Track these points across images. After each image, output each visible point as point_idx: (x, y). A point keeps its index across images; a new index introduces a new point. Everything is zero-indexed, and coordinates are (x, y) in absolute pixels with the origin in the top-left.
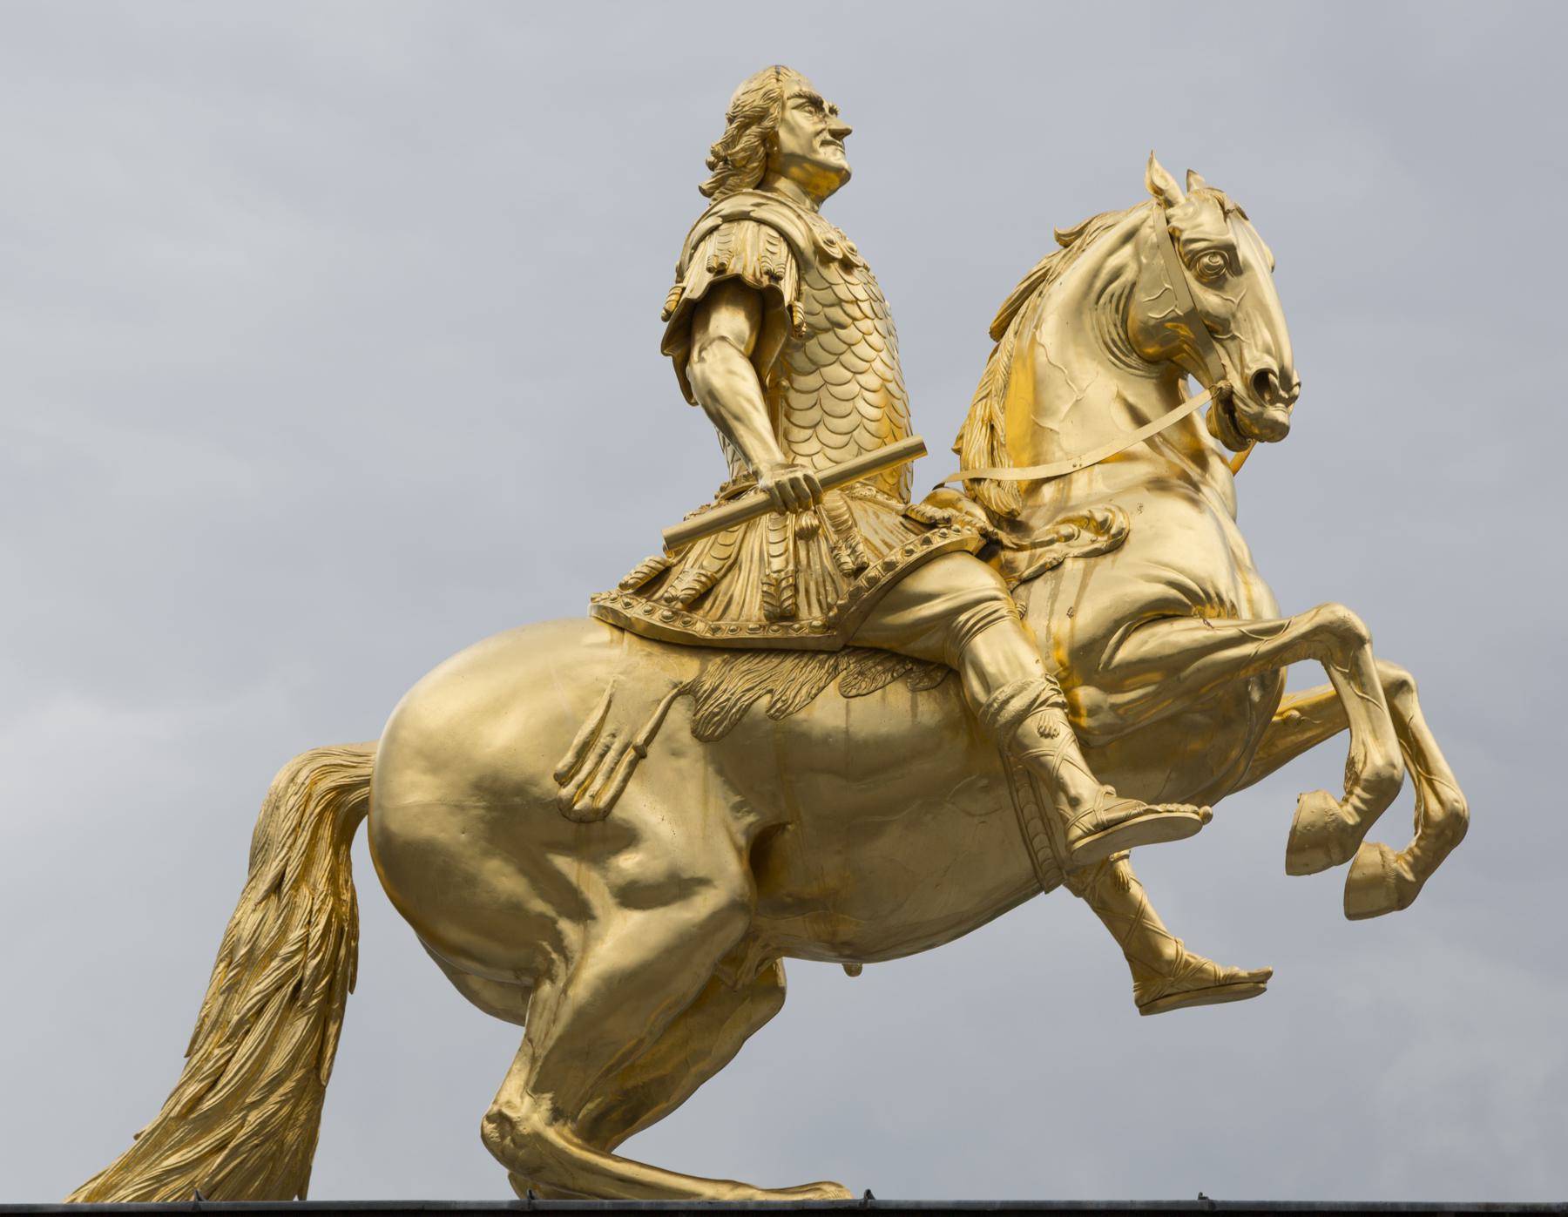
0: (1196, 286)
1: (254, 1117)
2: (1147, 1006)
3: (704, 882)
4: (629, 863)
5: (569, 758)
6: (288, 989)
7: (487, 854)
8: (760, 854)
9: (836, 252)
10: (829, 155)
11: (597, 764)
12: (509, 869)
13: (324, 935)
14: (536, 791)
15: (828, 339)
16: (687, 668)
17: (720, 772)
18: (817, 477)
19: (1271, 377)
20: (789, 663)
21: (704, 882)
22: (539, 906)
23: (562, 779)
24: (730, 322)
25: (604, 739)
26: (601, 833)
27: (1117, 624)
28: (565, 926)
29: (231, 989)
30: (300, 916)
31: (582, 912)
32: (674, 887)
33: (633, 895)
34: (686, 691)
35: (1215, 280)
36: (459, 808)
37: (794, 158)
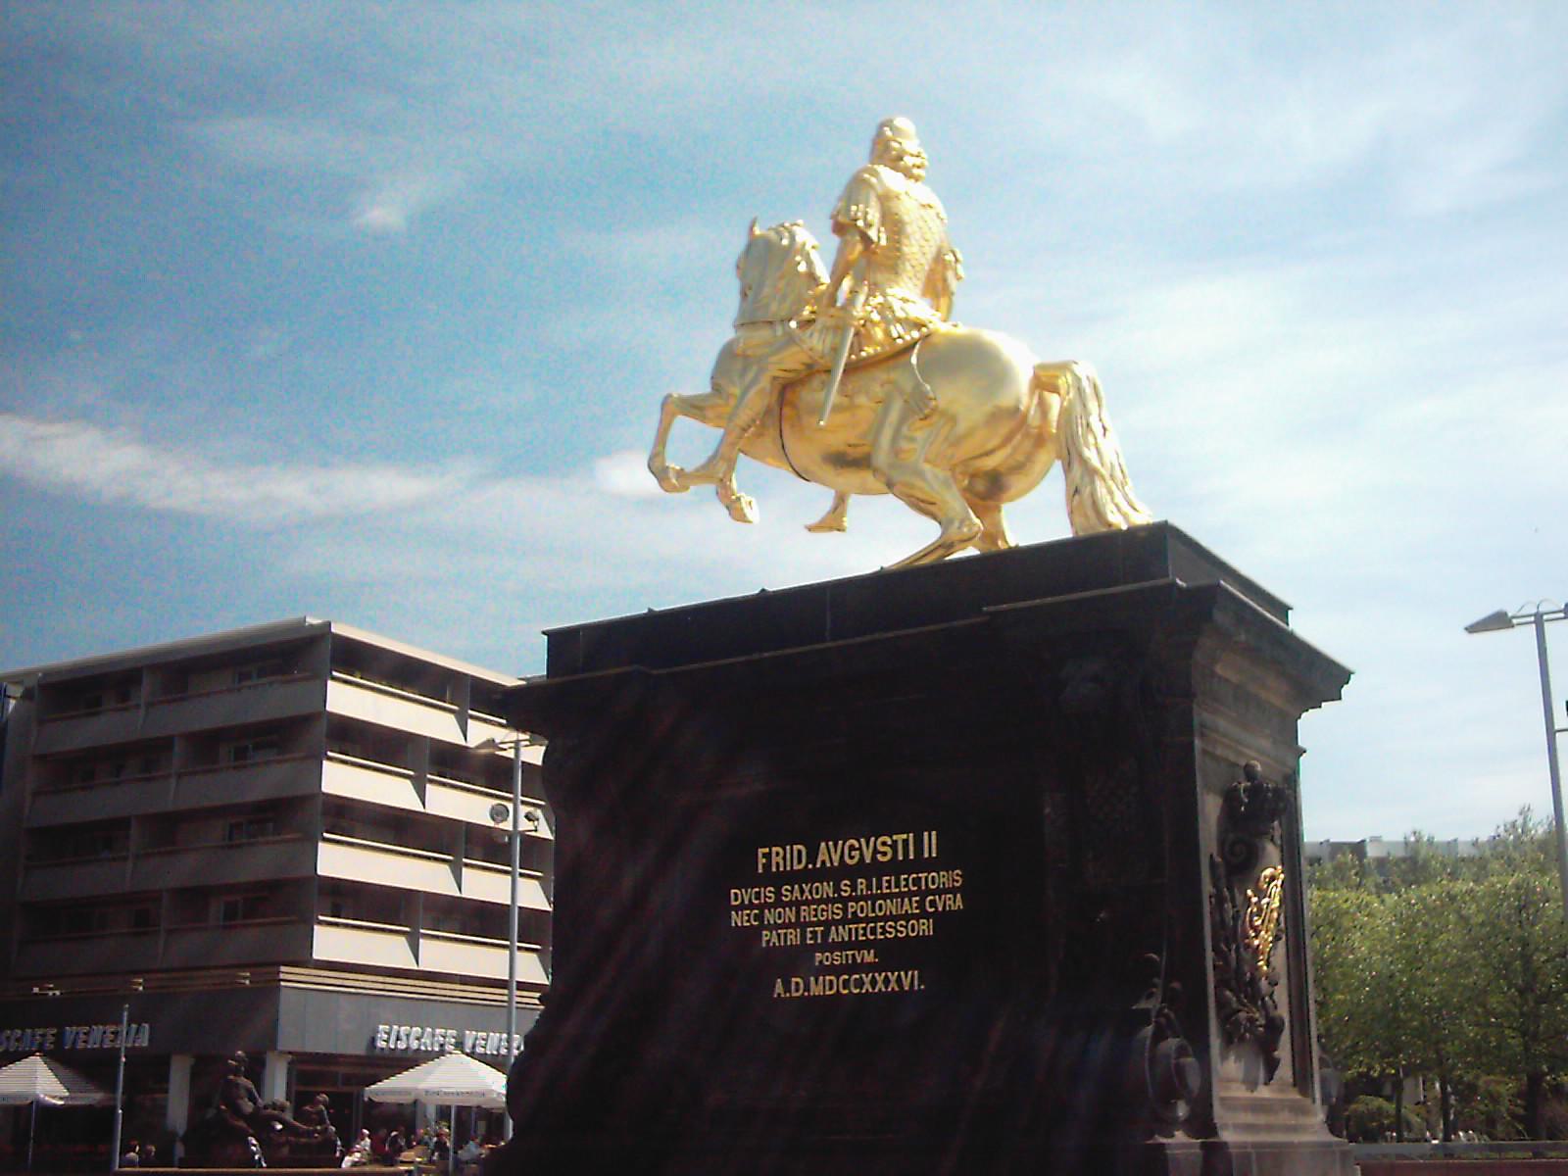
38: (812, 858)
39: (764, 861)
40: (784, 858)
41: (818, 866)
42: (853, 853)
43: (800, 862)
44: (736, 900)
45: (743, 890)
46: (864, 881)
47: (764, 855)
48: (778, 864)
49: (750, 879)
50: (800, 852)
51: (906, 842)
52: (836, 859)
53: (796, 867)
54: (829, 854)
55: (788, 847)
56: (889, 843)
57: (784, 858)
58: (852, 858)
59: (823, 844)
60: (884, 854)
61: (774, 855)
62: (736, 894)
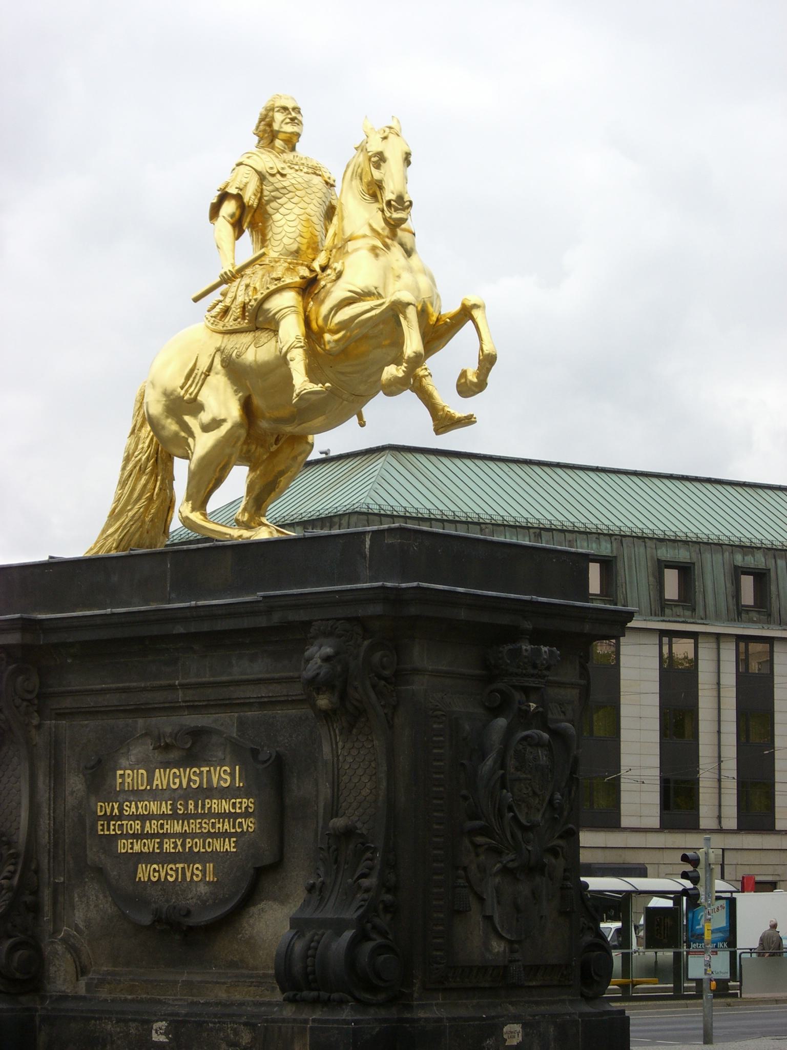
0: (372, 168)
1: (131, 514)
2: (437, 434)
3: (224, 420)
4: (205, 417)
5: (183, 380)
6: (138, 468)
7: (167, 417)
8: (247, 406)
9: (275, 171)
10: (289, 128)
11: (193, 382)
12: (174, 422)
13: (149, 447)
14: (176, 393)
15: (274, 204)
16: (218, 341)
17: (229, 379)
18: (234, 271)
19: (393, 203)
20: (243, 334)
21: (224, 420)
22: (183, 434)
23: (182, 388)
24: (229, 208)
25: (196, 371)
26: (195, 407)
27: (332, 309)
28: (190, 440)
29: (124, 468)
30: (141, 441)
31: (192, 434)
32: (215, 424)
33: (206, 428)
34: (218, 350)
35: (378, 166)
36: (158, 401)
37: (278, 132)
38: (150, 781)
39: (120, 781)
42: (177, 780)
49: (112, 795)
52: (165, 783)
53: (141, 788)
54: (161, 778)
60: (195, 782)
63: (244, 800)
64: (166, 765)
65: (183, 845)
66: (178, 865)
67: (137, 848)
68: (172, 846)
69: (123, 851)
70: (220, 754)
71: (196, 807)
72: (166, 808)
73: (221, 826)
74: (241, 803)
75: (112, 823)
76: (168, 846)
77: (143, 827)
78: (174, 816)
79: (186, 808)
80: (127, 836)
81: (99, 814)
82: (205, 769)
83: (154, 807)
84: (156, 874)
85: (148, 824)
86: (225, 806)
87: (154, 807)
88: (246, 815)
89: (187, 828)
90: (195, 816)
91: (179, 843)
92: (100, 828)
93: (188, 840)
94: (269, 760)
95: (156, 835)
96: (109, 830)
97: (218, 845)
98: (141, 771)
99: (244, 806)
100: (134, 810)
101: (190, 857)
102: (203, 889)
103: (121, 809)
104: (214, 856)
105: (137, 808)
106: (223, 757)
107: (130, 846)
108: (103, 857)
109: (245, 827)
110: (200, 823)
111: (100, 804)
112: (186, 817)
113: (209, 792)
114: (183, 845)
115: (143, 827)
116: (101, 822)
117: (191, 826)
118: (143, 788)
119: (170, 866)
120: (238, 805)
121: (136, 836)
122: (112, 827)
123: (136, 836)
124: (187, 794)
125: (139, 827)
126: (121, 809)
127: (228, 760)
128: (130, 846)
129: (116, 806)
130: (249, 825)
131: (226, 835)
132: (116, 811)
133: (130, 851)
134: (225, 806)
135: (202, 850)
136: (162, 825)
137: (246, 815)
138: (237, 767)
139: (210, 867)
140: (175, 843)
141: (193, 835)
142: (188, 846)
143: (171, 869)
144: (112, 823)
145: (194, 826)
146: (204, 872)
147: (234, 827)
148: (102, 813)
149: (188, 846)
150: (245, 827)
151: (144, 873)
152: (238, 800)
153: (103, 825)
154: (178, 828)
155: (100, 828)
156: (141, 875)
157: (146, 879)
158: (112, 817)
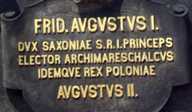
38: (68, 25)
39: (39, 26)
40: (51, 26)
41: (72, 31)
43: (60, 29)
44: (21, 48)
45: (26, 43)
46: (110, 40)
47: (39, 23)
48: (47, 28)
50: (60, 22)
51: (125, 20)
53: (58, 31)
54: (78, 25)
55: (53, 20)
56: (115, 19)
57: (51, 26)
58: (92, 28)
59: (75, 19)
61: (44, 23)
62: (21, 45)
63: (160, 39)
64: (83, 15)
65: (103, 71)
66: (98, 86)
67: (57, 74)
68: (92, 72)
69: (43, 77)
70: (134, 8)
71: (114, 44)
72: (85, 45)
73: (139, 57)
74: (158, 41)
75: (31, 57)
76: (88, 72)
77: (62, 59)
78: (94, 50)
79: (104, 44)
80: (47, 66)
81: (20, 50)
82: (121, 18)
83: (73, 45)
84: (77, 93)
85: (67, 56)
86: (144, 43)
87: (73, 45)
88: (164, 48)
89: (106, 59)
90: (114, 51)
91: (100, 70)
92: (20, 60)
93: (107, 68)
94: (183, 12)
95: (77, 65)
96: (28, 61)
97: (137, 70)
98: (58, 20)
99: (160, 43)
100: (53, 47)
101: (111, 79)
102: (123, 102)
103: (39, 46)
104: (133, 78)
105: (56, 45)
106: (137, 10)
107: (50, 73)
108: (23, 82)
109: (163, 58)
110: (119, 56)
111: (20, 43)
112: (108, 51)
113: (126, 34)
114: (103, 71)
115: (62, 59)
116: (20, 57)
117: (110, 58)
118: (62, 31)
119: (91, 86)
120: (154, 43)
121: (56, 66)
122: (31, 60)
123: (56, 66)
124: (104, 35)
125: (59, 59)
126: (39, 46)
127: (142, 10)
128: (50, 73)
129: (35, 45)
130: (169, 56)
131: (149, 64)
132: (35, 48)
133: (50, 77)
134: (144, 43)
135: (124, 75)
136: (82, 58)
137: (164, 48)
138: (152, 17)
139: (131, 87)
140: (95, 70)
141: (112, 64)
142: (108, 72)
143: (93, 89)
144: (31, 57)
145: (112, 57)
146: (125, 90)
147: (152, 57)
148: (22, 49)
149: (108, 72)
150: (163, 58)
151: (63, 92)
152: (154, 39)
153: (23, 59)
154: (97, 59)
155: (20, 60)
156: (63, 94)
157: (68, 97)
158: (30, 52)
